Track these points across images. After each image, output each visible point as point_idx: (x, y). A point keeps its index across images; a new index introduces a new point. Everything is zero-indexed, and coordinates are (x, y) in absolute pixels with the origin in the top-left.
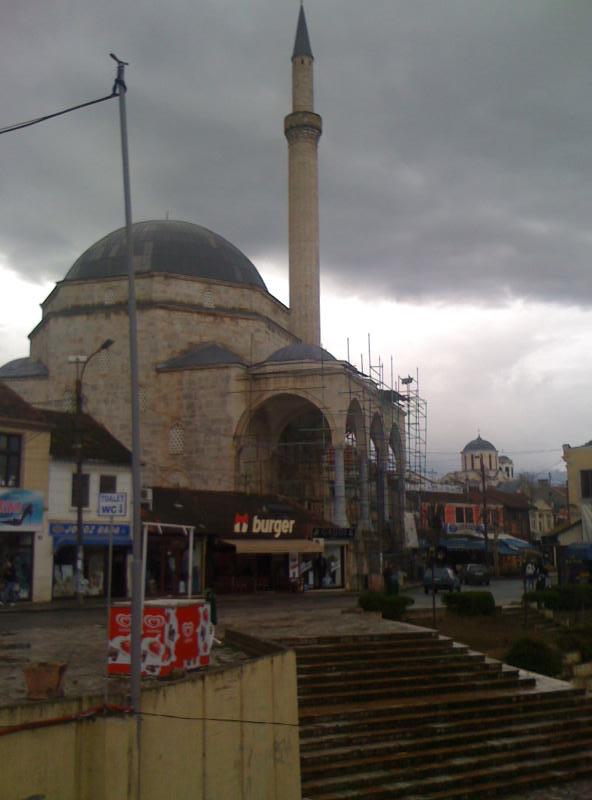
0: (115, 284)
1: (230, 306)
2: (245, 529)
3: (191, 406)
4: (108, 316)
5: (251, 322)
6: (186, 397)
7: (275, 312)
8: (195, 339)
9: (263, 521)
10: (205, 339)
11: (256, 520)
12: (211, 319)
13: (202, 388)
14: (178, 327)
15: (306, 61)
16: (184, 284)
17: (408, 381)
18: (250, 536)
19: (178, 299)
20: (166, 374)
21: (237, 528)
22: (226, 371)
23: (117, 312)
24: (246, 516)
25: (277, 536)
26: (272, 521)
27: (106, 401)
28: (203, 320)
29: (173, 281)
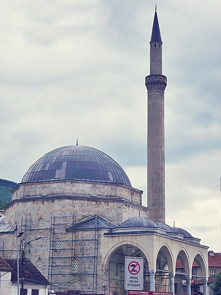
0: (47, 185)
1: (106, 194)
4: (43, 202)
7: (132, 194)
10: (91, 213)
14: (77, 208)
15: (157, 45)
23: (47, 201)
29: (76, 184)
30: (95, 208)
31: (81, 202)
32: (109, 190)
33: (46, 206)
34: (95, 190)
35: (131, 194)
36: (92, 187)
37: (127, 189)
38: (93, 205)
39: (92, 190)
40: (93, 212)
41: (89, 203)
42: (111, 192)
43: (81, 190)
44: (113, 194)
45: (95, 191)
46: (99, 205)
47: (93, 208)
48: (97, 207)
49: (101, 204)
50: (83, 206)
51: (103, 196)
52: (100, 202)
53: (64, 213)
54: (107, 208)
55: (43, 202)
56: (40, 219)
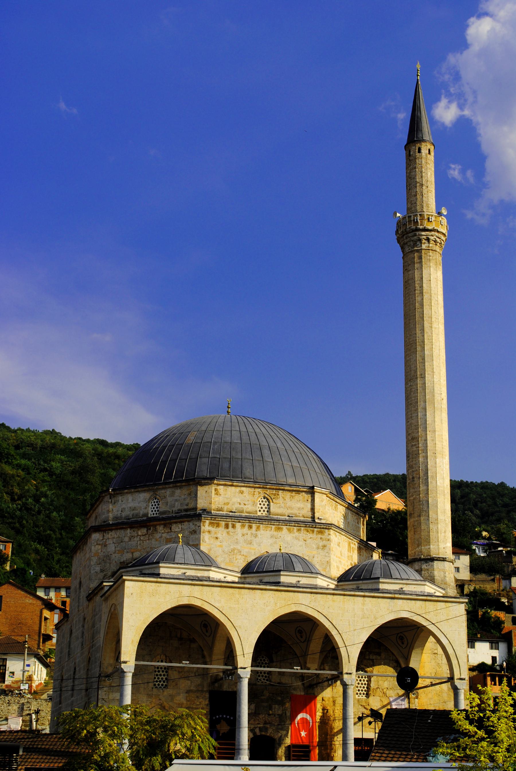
1: (178, 506)
5: (186, 523)
12: (144, 531)
16: (130, 497)
19: (124, 515)
30: (145, 542)
31: (118, 534)
32: (183, 497)
34: (157, 502)
35: (264, 498)
36: (150, 498)
38: (140, 536)
39: (153, 503)
40: (140, 551)
42: (186, 502)
43: (130, 507)
44: (191, 506)
45: (158, 505)
47: (142, 541)
48: (148, 539)
49: (156, 530)
50: (122, 542)
51: (172, 512)
54: (168, 537)
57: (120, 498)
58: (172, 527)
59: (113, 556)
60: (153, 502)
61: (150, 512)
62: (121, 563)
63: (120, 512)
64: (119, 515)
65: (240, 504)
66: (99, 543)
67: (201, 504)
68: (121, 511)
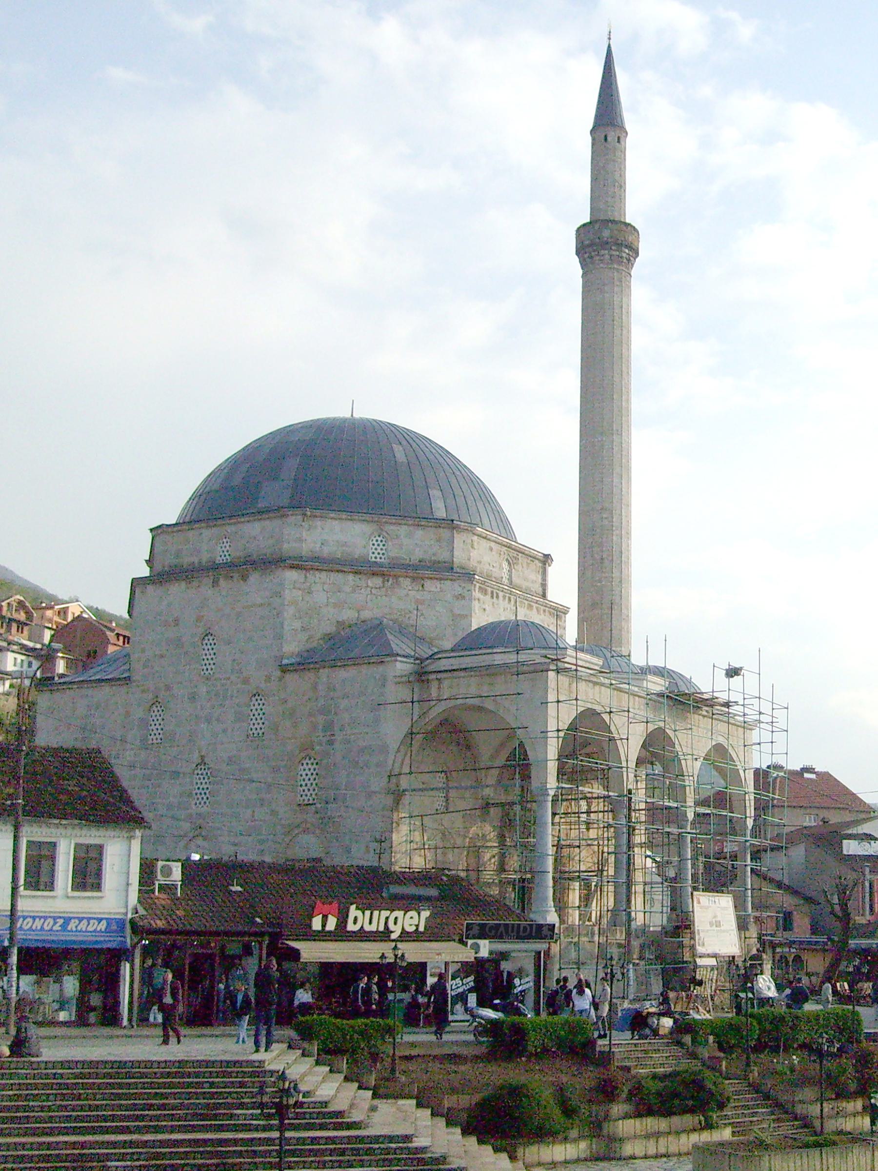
0: (231, 529)
1: (418, 555)
2: (332, 923)
3: (329, 726)
5: (448, 583)
6: (323, 711)
8: (348, 615)
9: (368, 913)
10: (366, 614)
11: (353, 911)
12: (378, 581)
13: (346, 696)
17: (733, 672)
18: (341, 934)
19: (326, 551)
20: (295, 676)
21: (316, 924)
22: (381, 668)
24: (335, 905)
25: (394, 936)
26: (385, 913)
27: (209, 721)
28: (363, 583)
29: (318, 523)
31: (332, 579)
33: (224, 593)
35: (507, 560)
37: (493, 544)
39: (374, 542)
41: (358, 582)
43: (337, 541)
46: (392, 587)
48: (386, 596)
49: (398, 583)
50: (339, 592)
52: (396, 577)
53: (275, 612)
55: (215, 583)
56: (207, 635)
57: (319, 523)
58: (425, 584)
59: (324, 611)
60: (375, 539)
61: (371, 555)
62: (338, 622)
63: (318, 545)
64: (318, 549)
65: (489, 564)
66: (297, 586)
67: (459, 557)
68: (322, 544)
